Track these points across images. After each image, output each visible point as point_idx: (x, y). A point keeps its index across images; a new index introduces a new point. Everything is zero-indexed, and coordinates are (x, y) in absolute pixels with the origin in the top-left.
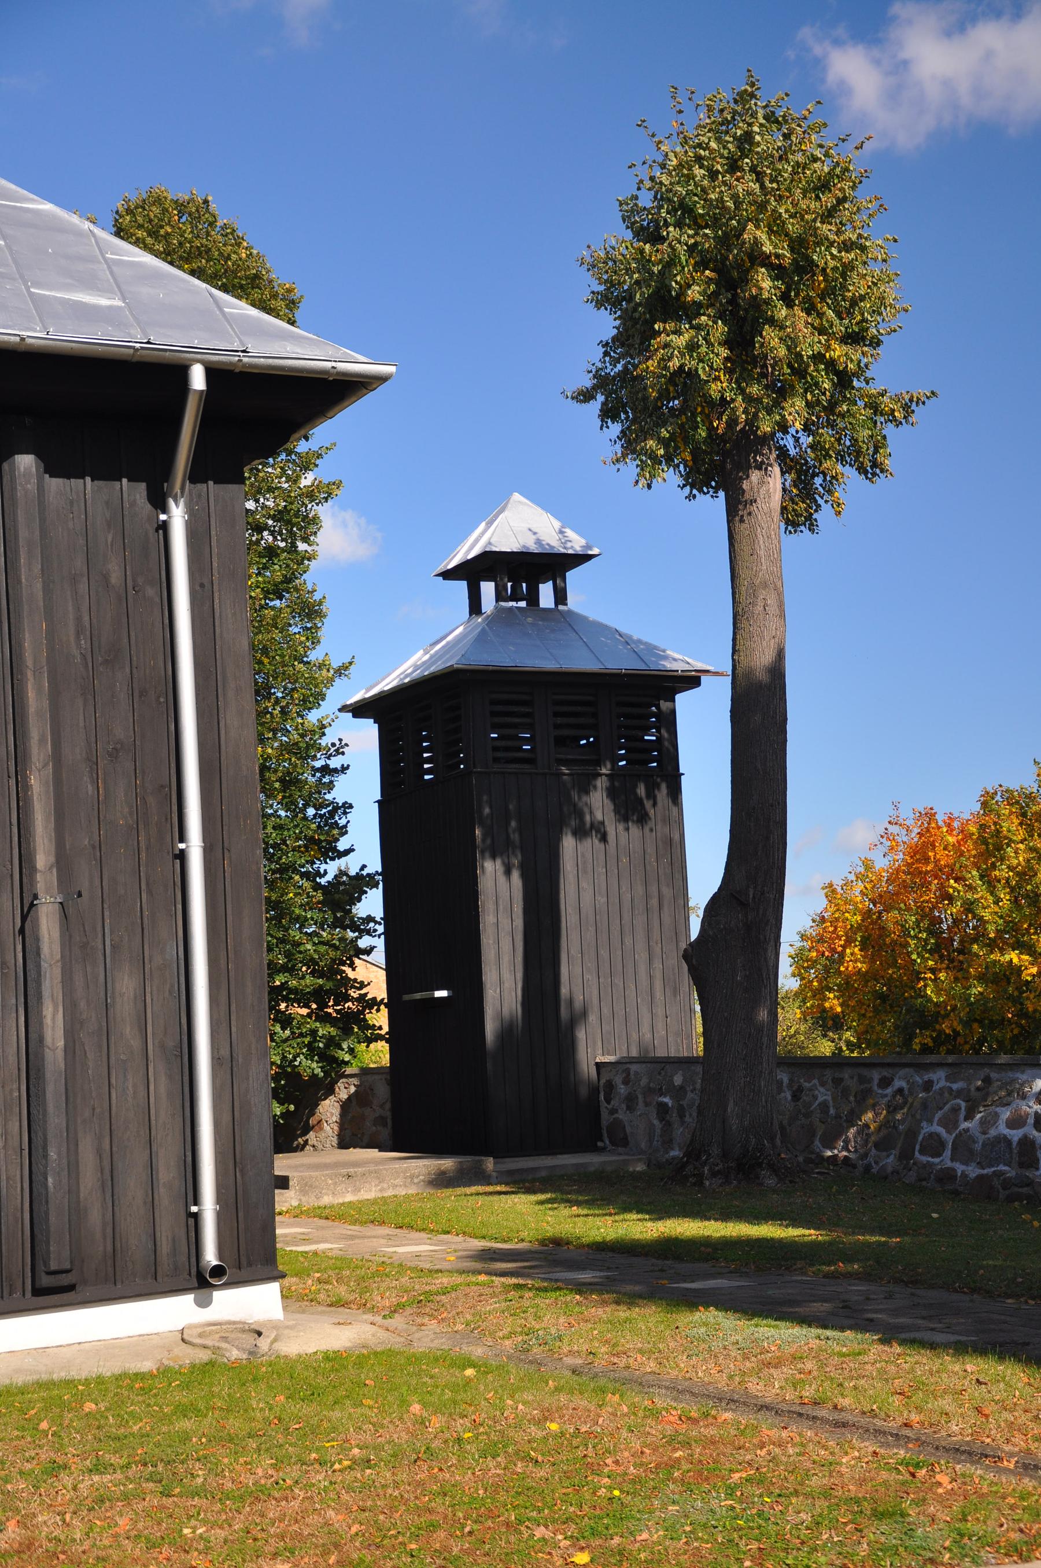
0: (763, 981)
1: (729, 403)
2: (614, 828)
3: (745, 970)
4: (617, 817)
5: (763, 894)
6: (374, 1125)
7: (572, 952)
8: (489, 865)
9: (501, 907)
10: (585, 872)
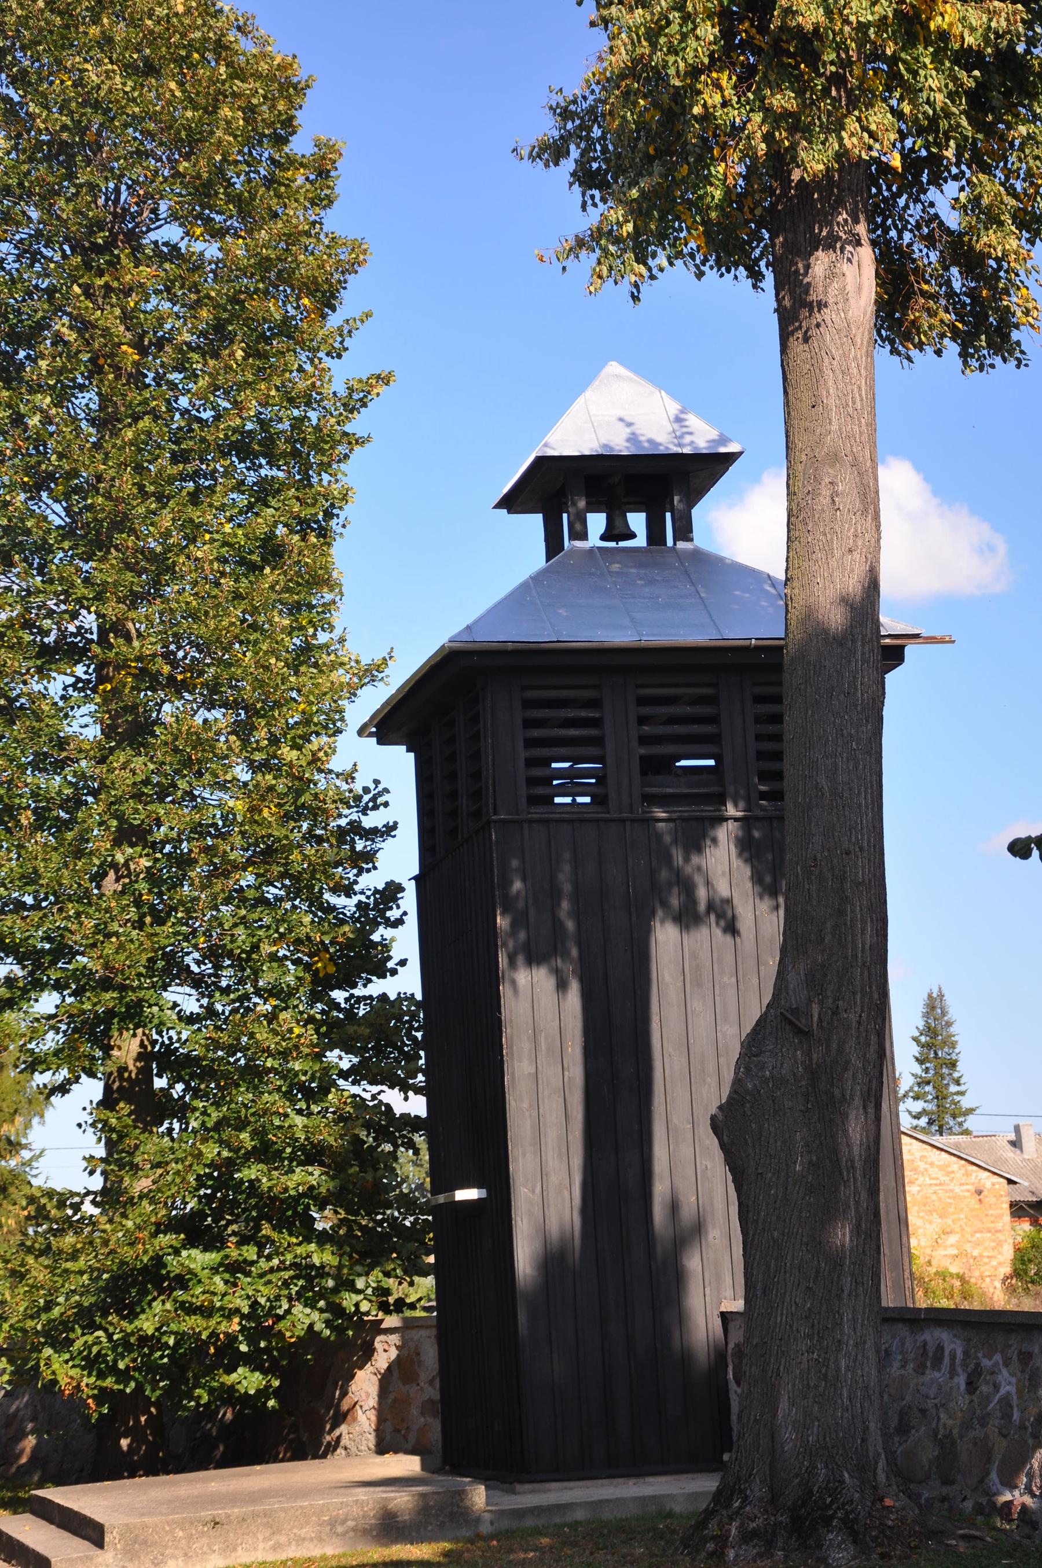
0: (841, 1173)
1: (743, 128)
2: (751, 907)
3: (809, 1152)
4: (758, 889)
5: (836, 1012)
6: (423, 1414)
7: (675, 1120)
8: (523, 977)
9: (543, 1046)
10: (700, 985)
